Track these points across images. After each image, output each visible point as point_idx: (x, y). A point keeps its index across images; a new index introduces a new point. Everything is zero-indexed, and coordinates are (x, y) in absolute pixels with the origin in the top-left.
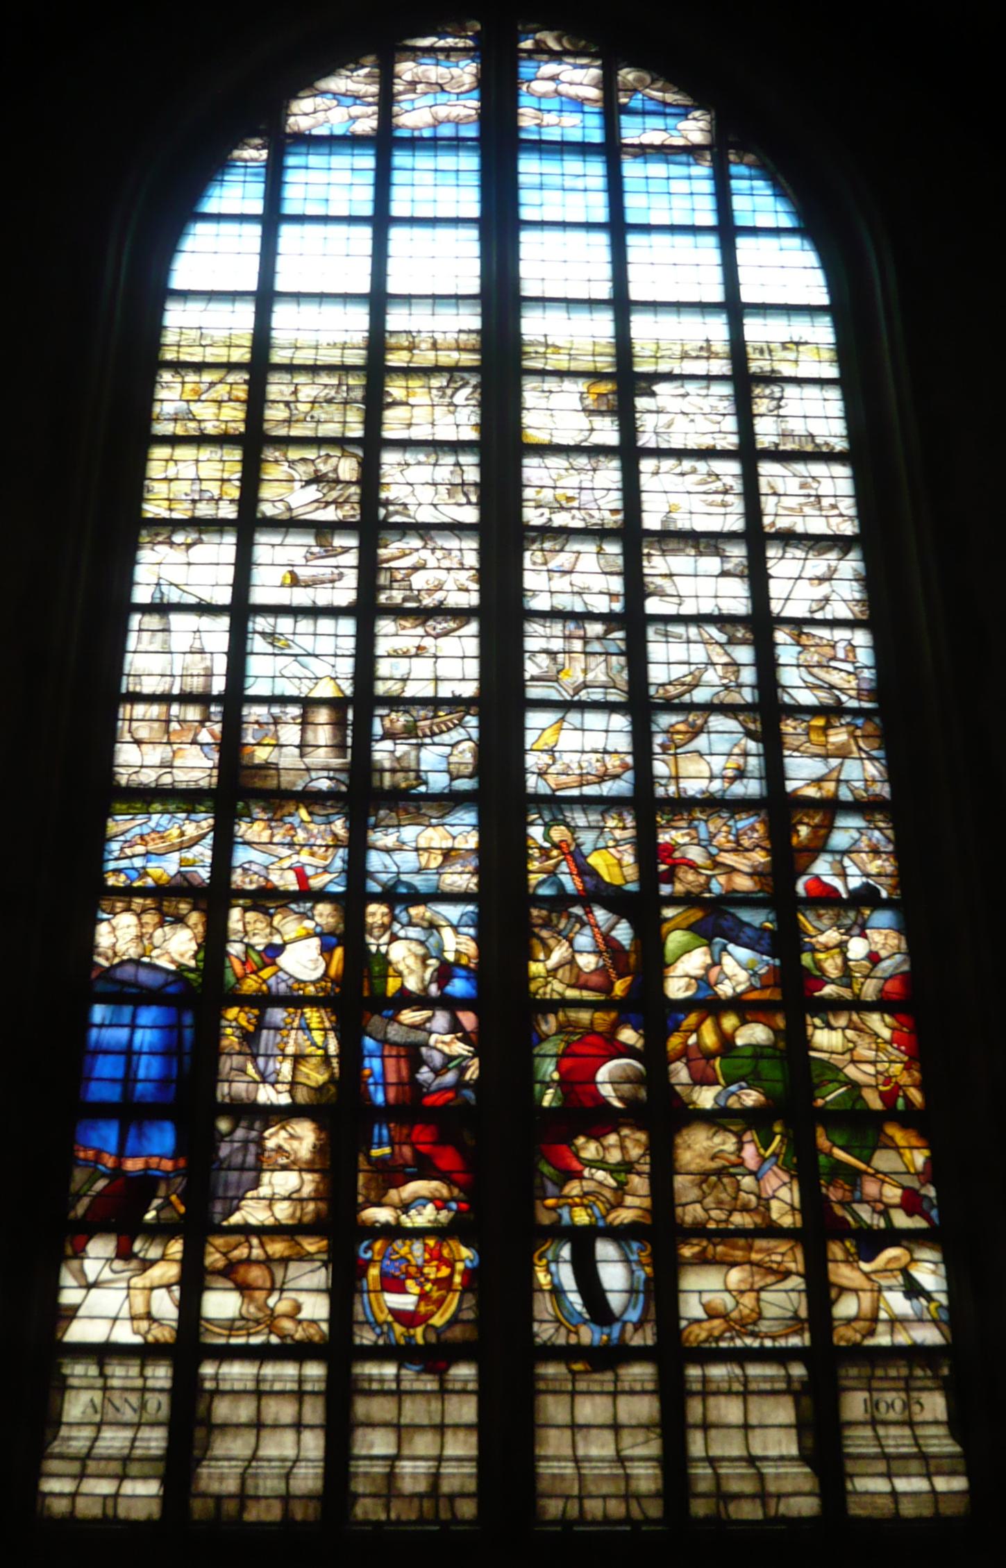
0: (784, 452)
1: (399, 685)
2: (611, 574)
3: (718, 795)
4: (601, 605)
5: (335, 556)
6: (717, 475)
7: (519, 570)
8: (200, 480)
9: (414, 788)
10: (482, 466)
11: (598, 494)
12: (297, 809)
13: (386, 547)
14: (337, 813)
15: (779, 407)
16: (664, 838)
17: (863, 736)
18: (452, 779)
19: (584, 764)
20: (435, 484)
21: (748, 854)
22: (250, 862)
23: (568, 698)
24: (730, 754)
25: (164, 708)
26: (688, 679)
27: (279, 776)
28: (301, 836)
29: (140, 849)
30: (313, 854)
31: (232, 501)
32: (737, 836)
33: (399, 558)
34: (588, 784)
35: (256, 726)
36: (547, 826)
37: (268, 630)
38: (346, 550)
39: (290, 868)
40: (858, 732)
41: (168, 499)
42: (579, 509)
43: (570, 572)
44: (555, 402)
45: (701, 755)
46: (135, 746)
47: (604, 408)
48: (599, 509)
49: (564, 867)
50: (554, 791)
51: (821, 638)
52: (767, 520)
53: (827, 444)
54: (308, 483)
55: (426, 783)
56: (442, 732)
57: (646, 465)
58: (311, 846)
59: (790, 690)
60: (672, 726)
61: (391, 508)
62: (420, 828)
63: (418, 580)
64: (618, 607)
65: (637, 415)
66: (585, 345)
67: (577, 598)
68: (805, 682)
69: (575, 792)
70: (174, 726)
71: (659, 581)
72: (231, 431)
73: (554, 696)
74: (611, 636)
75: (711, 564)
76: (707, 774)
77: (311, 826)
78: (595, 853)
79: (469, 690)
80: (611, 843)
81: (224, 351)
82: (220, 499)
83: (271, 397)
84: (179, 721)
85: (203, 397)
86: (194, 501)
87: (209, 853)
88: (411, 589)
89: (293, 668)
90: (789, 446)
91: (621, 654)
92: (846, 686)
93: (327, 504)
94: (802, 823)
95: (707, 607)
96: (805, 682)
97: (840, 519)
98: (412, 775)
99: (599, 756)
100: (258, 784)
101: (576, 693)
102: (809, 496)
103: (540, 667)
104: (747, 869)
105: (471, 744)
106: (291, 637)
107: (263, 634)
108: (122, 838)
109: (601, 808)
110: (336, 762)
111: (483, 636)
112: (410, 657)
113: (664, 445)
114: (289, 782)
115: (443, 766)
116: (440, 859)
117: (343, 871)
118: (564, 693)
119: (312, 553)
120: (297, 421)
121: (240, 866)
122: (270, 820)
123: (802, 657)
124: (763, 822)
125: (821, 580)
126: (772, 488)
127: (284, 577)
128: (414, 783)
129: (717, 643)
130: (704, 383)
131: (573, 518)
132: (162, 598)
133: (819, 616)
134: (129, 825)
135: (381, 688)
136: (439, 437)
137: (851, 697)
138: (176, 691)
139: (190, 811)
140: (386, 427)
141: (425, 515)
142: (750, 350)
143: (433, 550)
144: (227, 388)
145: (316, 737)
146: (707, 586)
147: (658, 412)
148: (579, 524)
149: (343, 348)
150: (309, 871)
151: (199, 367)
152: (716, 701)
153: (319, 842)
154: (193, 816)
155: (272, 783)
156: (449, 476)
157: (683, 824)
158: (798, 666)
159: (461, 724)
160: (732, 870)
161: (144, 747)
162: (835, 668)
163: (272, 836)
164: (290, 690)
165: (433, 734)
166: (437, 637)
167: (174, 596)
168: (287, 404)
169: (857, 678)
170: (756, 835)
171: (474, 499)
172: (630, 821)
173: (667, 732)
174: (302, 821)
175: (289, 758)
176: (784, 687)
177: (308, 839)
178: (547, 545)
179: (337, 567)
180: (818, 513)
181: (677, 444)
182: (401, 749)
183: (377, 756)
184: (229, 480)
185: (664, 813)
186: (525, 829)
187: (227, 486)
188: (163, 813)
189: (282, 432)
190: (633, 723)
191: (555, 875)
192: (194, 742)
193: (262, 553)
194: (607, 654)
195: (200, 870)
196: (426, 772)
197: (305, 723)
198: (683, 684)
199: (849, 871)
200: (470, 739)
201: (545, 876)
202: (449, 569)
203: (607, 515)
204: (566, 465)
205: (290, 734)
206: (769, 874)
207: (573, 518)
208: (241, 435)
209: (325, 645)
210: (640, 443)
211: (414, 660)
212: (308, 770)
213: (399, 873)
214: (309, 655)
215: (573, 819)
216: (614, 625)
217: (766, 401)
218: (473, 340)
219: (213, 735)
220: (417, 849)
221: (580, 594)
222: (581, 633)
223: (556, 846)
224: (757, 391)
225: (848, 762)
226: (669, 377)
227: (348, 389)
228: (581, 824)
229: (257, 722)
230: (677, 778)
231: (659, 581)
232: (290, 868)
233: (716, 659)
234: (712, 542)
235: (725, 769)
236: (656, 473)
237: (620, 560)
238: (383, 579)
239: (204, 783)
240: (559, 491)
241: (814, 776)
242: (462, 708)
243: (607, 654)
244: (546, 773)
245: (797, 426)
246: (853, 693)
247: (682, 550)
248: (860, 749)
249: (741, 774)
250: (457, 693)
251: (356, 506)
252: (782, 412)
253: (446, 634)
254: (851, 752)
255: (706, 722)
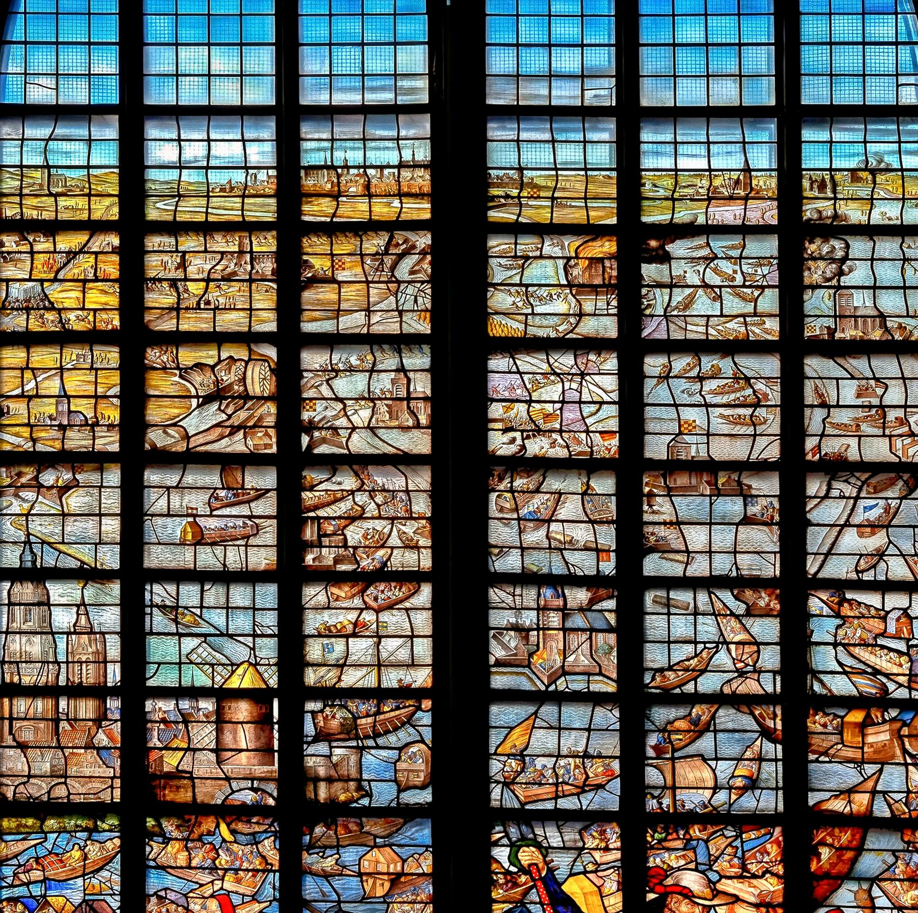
0: (842, 341)
1: (334, 673)
2: (601, 522)
3: (723, 810)
4: (584, 564)
5: (248, 502)
6: (747, 379)
7: (483, 519)
8: (68, 397)
9: (356, 801)
10: (434, 371)
11: (587, 409)
12: (218, 826)
13: (311, 489)
14: (265, 831)
15: (841, 273)
16: (654, 861)
17: (908, 736)
18: (400, 790)
19: (561, 772)
20: (373, 400)
21: (754, 882)
22: (166, 889)
23: (543, 688)
24: (739, 760)
25: (50, 702)
26: (693, 662)
27: (194, 787)
28: (224, 859)
29: (37, 875)
30: (238, 881)
31: (111, 427)
32: (743, 859)
33: (329, 504)
34: (564, 796)
35: (162, 726)
36: (515, 847)
37: (168, 603)
38: (261, 494)
39: (212, 896)
40: (905, 731)
41: (28, 425)
42: (561, 431)
43: (549, 521)
44: (537, 272)
45: (705, 760)
46: (19, 751)
47: (598, 281)
48: (587, 432)
49: (533, 896)
50: (523, 804)
51: (868, 607)
52: (810, 443)
53: (900, 327)
54: (208, 400)
55: (369, 795)
56: (387, 732)
57: (653, 364)
58: (236, 871)
59: (822, 676)
60: (671, 723)
61: (316, 434)
62: (362, 850)
63: (354, 534)
64: (608, 567)
65: (644, 291)
66: (573, 183)
67: (556, 558)
68: (841, 664)
69: (549, 806)
70: (64, 725)
71: (662, 531)
72: (101, 326)
73: (526, 686)
74: (595, 607)
75: (733, 507)
76: (711, 784)
77: (235, 847)
78: (571, 879)
79: (422, 678)
80: (590, 867)
81: (82, 202)
82: (97, 424)
83: (151, 274)
84: (68, 720)
85: (60, 276)
86: (62, 428)
87: (116, 878)
88: (345, 546)
89: (204, 652)
90: (849, 332)
91: (610, 630)
92: (896, 670)
93: (234, 430)
94: (823, 843)
95: (722, 565)
96: (841, 664)
97: (909, 440)
98: (352, 785)
99: (577, 760)
100: (170, 796)
101: (555, 682)
102: (870, 407)
103: (505, 647)
104: (752, 899)
105: (422, 746)
106: (198, 611)
107: (163, 608)
108: (15, 862)
109: (579, 826)
110: (261, 770)
111: (437, 607)
112: (347, 637)
113: (677, 335)
114: (205, 794)
115: (389, 775)
116: (387, 885)
117: (275, 899)
118: (538, 683)
119: (217, 499)
120: (187, 309)
121: (155, 893)
122: (187, 840)
123: (841, 632)
124: (777, 842)
125: (873, 527)
126: (821, 396)
127: (184, 531)
128: (354, 794)
129: (732, 614)
130: (736, 240)
131: (553, 444)
132: (34, 562)
133: (868, 576)
134: (21, 846)
135: (311, 677)
136: (377, 329)
137: (900, 685)
138: (62, 682)
139: (92, 831)
140: (306, 315)
141: (359, 444)
142: (806, 184)
143: (372, 493)
144: (92, 259)
145: (235, 738)
146: (723, 537)
147: (671, 286)
148: (562, 453)
149: (243, 196)
150: (236, 899)
151: (52, 228)
152: (727, 690)
153: (245, 865)
154: (96, 836)
155: (184, 796)
156: (389, 386)
157: (679, 844)
158: (835, 645)
159: (409, 721)
160: (736, 899)
161: (30, 752)
162: (883, 647)
163: (190, 859)
164: (202, 680)
165: (376, 735)
166: (378, 611)
167: (49, 560)
168: (173, 283)
169: (911, 661)
170: (766, 859)
171: (423, 420)
172: (614, 842)
173: (664, 730)
174: (224, 840)
175: (205, 764)
176: (815, 674)
177: (233, 862)
178: (519, 483)
179: (250, 517)
180: (880, 432)
181: (696, 331)
182: (337, 751)
183: (310, 762)
184: (105, 397)
185: (655, 831)
186: (490, 851)
187: (102, 404)
188: (59, 832)
189: (168, 325)
190: (621, 719)
191: (524, 905)
192: (89, 746)
193: (155, 501)
194: (592, 630)
195: (108, 899)
196: (369, 781)
197: (220, 720)
198: (686, 670)
199: (878, 903)
200: (422, 741)
201: (511, 906)
202: (393, 519)
203: (597, 438)
204: (545, 367)
205: (204, 735)
206: (779, 905)
207: (553, 444)
208: (114, 331)
209: (242, 623)
210: (645, 334)
211: (350, 640)
212: (228, 779)
213: (339, 902)
214: (222, 635)
215: (546, 838)
216: (602, 592)
217: (822, 264)
218: (422, 180)
219: (111, 738)
220: (360, 875)
221: (561, 550)
222: (560, 602)
223: (523, 870)
224: (812, 248)
225: (886, 767)
226: (689, 230)
227: (252, 260)
228: (555, 845)
229: (163, 721)
230: (674, 788)
231: (662, 531)
232: (212, 896)
233: (730, 637)
234: (735, 476)
235: (733, 776)
236: (665, 377)
237: (613, 506)
238: (309, 533)
239: (106, 797)
240: (537, 406)
241: (844, 786)
242: (411, 702)
243: (592, 630)
244: (513, 782)
245: (861, 301)
246: (903, 680)
247: (695, 488)
248: (905, 751)
249: (752, 784)
250: (408, 680)
251: (272, 432)
252: (845, 281)
253: (390, 607)
254: (893, 756)
255: (713, 717)
